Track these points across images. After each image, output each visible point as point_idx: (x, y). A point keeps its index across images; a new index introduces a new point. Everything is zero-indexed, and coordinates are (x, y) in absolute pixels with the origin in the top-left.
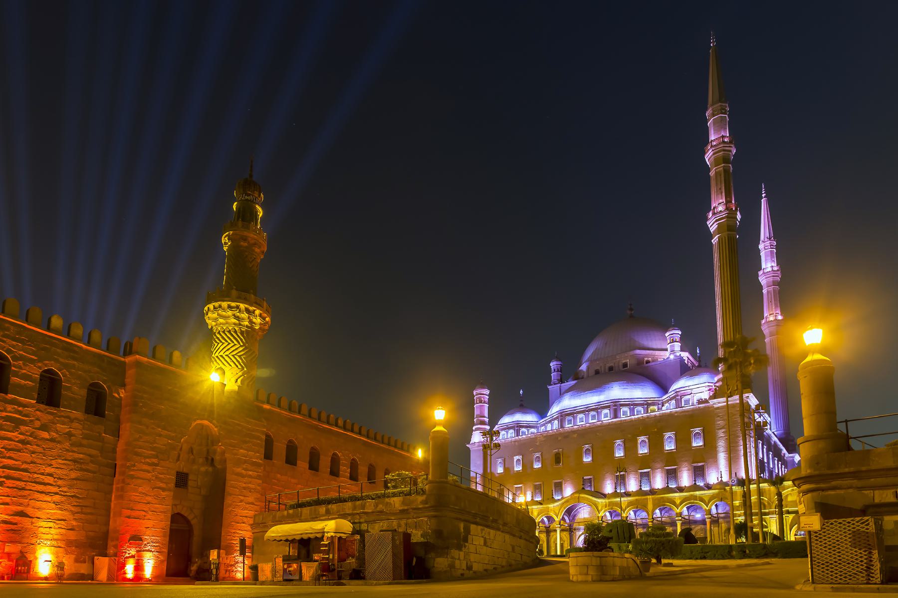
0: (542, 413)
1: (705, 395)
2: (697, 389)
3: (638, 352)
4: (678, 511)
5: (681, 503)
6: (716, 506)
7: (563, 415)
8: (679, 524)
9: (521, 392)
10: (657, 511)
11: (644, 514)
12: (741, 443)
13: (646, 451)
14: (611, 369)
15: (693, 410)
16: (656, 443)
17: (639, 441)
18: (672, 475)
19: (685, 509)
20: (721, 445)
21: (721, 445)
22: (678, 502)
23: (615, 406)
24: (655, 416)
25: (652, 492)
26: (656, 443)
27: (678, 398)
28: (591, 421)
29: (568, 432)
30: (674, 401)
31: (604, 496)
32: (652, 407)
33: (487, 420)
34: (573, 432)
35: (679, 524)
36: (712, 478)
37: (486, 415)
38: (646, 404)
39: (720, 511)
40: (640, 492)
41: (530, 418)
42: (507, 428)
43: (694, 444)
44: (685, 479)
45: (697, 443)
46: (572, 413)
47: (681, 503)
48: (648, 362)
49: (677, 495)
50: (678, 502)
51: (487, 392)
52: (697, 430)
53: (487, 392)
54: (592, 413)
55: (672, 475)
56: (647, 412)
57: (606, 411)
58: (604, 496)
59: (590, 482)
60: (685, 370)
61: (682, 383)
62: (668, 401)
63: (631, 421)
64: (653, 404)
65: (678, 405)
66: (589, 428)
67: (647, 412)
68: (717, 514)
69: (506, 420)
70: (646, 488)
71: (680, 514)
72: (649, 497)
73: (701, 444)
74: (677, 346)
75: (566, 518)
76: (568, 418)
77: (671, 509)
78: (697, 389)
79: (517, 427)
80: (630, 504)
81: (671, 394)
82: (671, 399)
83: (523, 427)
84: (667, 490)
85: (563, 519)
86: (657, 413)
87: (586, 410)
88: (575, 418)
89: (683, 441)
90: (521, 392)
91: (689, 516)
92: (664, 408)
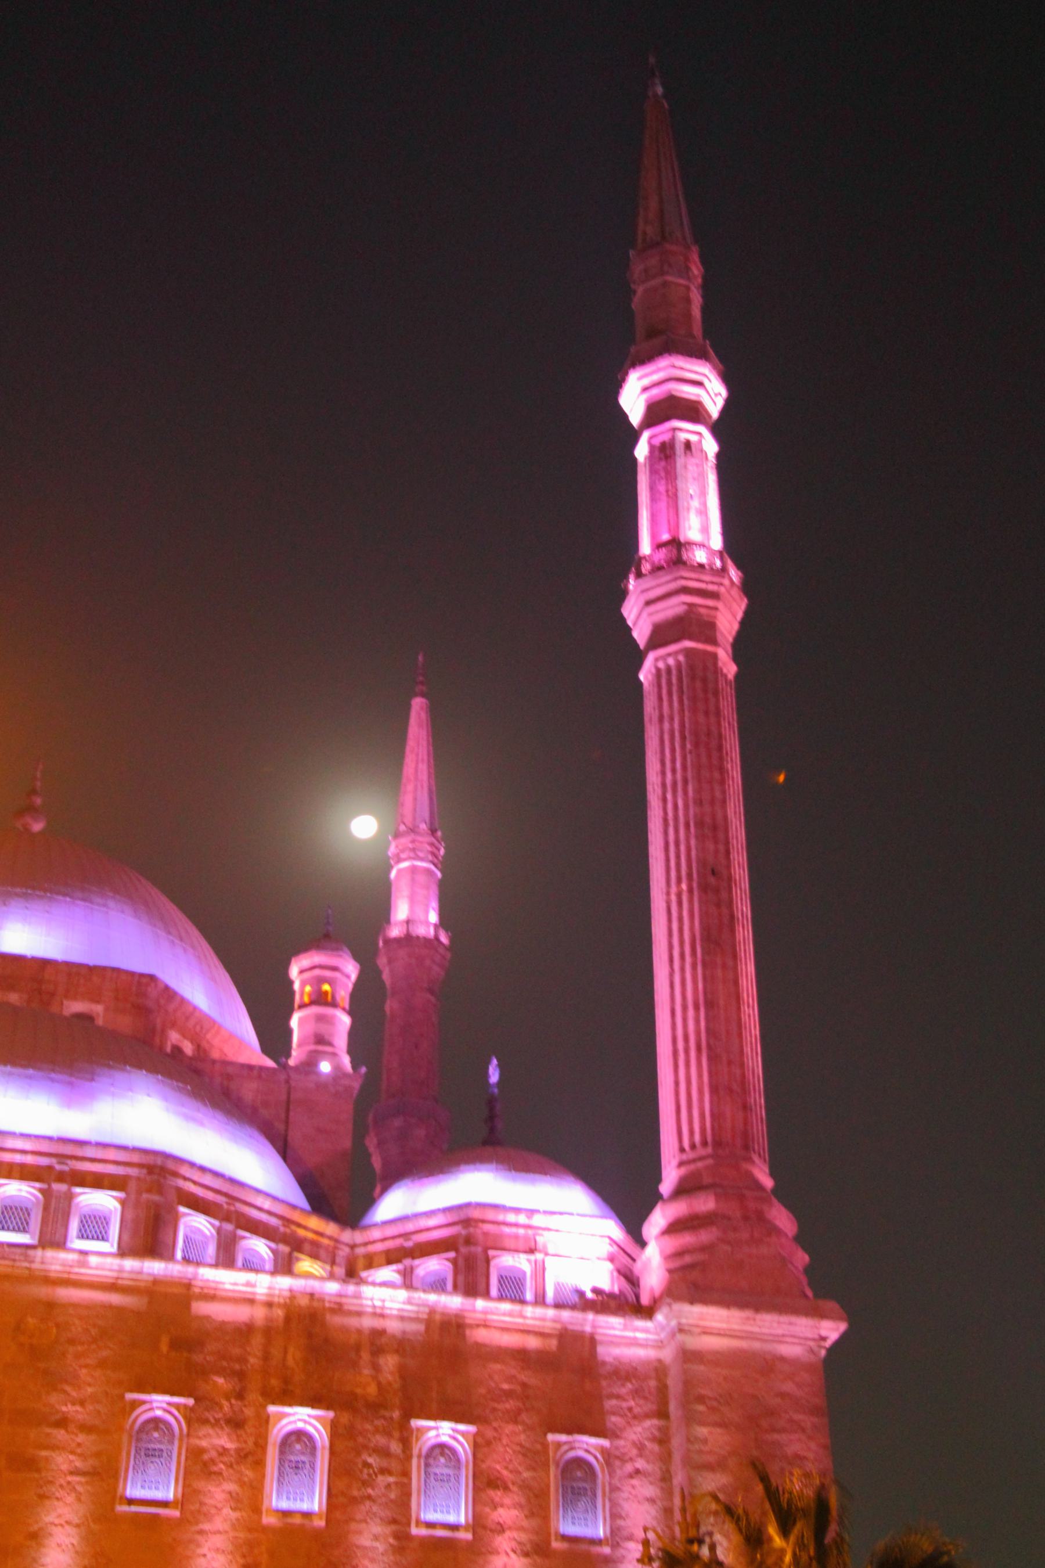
23: (156, 1191)
57: (103, 1201)
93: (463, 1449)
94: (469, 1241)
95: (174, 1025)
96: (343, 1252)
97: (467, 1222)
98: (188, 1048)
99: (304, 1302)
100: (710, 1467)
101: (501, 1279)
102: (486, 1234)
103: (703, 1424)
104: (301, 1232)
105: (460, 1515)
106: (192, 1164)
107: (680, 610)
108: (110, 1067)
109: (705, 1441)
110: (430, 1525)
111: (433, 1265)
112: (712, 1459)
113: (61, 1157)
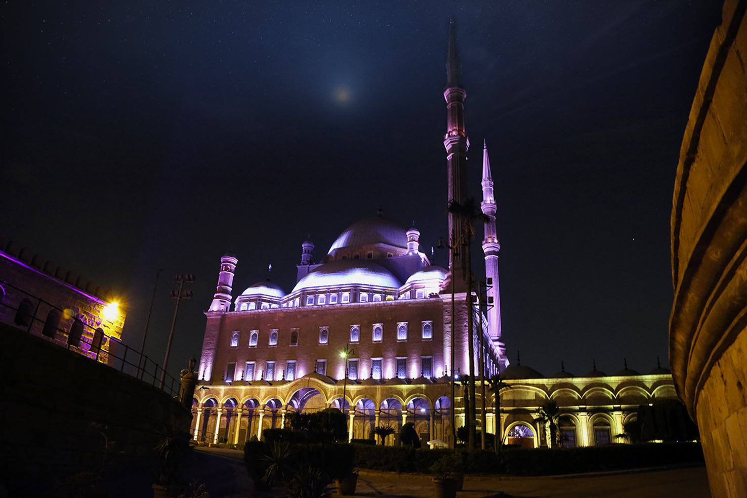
0: (287, 290)
1: (437, 290)
2: (430, 283)
3: (382, 245)
4: (404, 403)
5: (408, 395)
6: (440, 401)
7: (304, 293)
8: (404, 416)
9: (270, 267)
10: (385, 402)
11: (372, 405)
12: (467, 338)
13: (380, 339)
14: (357, 257)
15: (425, 303)
16: (390, 332)
17: (375, 328)
18: (402, 366)
19: (411, 402)
20: (448, 339)
21: (448, 339)
22: (405, 394)
23: (355, 290)
24: (391, 305)
25: (383, 381)
26: (390, 332)
27: (413, 290)
28: (331, 303)
29: (307, 311)
30: (408, 293)
31: (335, 382)
32: (389, 297)
33: (230, 289)
34: (312, 311)
35: (404, 416)
36: (439, 373)
37: (231, 284)
38: (385, 293)
39: (443, 407)
40: (371, 381)
41: (275, 293)
42: (249, 300)
43: (424, 337)
44: (414, 372)
45: (427, 336)
46: (315, 292)
47: (408, 395)
48: (390, 256)
49: (404, 387)
50: (405, 394)
51: (236, 261)
52: (427, 322)
53: (236, 261)
54: (334, 295)
55: (402, 366)
56: (385, 300)
57: (346, 294)
58: (335, 382)
59: (324, 367)
60: (416, 266)
61: (417, 277)
62: (404, 292)
63: (369, 307)
64: (390, 294)
65: (413, 296)
66: (329, 309)
67: (385, 300)
68: (441, 409)
69: (250, 291)
70: (376, 376)
71: (406, 408)
72: (378, 387)
73: (430, 337)
74: (416, 245)
75: (294, 402)
76: (309, 297)
77: (398, 402)
78: (430, 283)
79: (259, 300)
80: (359, 393)
81: (407, 285)
82: (406, 291)
83: (265, 301)
84: (396, 381)
85: (291, 403)
86: (393, 302)
87: (328, 291)
88: (316, 298)
89: (414, 331)
90: (270, 267)
91: (415, 409)
92: (399, 298)
93: (406, 326)
94: (412, 288)
95: (388, 251)
96: (397, 293)
97: (412, 284)
98: (392, 254)
99: (378, 305)
100: (448, 323)
101: (418, 294)
102: (415, 286)
103: (447, 316)
104: (387, 291)
105: (405, 338)
106: (362, 284)
107: (451, 146)
108: (352, 269)
109: (447, 319)
110: (400, 340)
111: (408, 293)
112: (448, 322)
113: (340, 288)
